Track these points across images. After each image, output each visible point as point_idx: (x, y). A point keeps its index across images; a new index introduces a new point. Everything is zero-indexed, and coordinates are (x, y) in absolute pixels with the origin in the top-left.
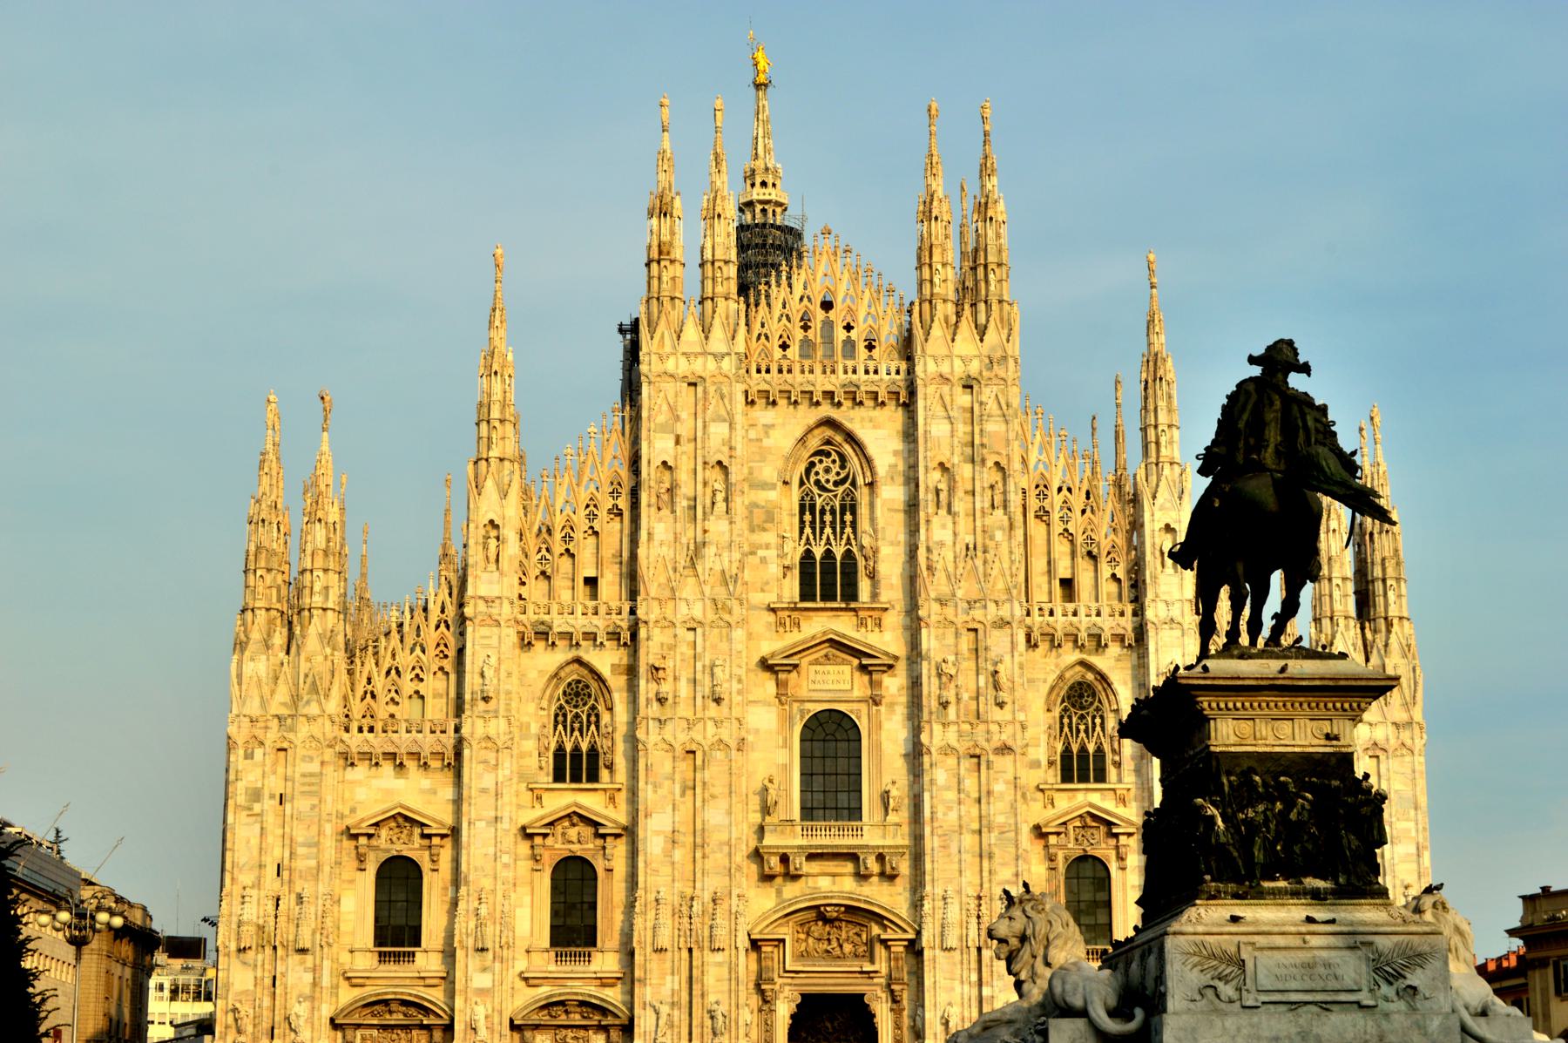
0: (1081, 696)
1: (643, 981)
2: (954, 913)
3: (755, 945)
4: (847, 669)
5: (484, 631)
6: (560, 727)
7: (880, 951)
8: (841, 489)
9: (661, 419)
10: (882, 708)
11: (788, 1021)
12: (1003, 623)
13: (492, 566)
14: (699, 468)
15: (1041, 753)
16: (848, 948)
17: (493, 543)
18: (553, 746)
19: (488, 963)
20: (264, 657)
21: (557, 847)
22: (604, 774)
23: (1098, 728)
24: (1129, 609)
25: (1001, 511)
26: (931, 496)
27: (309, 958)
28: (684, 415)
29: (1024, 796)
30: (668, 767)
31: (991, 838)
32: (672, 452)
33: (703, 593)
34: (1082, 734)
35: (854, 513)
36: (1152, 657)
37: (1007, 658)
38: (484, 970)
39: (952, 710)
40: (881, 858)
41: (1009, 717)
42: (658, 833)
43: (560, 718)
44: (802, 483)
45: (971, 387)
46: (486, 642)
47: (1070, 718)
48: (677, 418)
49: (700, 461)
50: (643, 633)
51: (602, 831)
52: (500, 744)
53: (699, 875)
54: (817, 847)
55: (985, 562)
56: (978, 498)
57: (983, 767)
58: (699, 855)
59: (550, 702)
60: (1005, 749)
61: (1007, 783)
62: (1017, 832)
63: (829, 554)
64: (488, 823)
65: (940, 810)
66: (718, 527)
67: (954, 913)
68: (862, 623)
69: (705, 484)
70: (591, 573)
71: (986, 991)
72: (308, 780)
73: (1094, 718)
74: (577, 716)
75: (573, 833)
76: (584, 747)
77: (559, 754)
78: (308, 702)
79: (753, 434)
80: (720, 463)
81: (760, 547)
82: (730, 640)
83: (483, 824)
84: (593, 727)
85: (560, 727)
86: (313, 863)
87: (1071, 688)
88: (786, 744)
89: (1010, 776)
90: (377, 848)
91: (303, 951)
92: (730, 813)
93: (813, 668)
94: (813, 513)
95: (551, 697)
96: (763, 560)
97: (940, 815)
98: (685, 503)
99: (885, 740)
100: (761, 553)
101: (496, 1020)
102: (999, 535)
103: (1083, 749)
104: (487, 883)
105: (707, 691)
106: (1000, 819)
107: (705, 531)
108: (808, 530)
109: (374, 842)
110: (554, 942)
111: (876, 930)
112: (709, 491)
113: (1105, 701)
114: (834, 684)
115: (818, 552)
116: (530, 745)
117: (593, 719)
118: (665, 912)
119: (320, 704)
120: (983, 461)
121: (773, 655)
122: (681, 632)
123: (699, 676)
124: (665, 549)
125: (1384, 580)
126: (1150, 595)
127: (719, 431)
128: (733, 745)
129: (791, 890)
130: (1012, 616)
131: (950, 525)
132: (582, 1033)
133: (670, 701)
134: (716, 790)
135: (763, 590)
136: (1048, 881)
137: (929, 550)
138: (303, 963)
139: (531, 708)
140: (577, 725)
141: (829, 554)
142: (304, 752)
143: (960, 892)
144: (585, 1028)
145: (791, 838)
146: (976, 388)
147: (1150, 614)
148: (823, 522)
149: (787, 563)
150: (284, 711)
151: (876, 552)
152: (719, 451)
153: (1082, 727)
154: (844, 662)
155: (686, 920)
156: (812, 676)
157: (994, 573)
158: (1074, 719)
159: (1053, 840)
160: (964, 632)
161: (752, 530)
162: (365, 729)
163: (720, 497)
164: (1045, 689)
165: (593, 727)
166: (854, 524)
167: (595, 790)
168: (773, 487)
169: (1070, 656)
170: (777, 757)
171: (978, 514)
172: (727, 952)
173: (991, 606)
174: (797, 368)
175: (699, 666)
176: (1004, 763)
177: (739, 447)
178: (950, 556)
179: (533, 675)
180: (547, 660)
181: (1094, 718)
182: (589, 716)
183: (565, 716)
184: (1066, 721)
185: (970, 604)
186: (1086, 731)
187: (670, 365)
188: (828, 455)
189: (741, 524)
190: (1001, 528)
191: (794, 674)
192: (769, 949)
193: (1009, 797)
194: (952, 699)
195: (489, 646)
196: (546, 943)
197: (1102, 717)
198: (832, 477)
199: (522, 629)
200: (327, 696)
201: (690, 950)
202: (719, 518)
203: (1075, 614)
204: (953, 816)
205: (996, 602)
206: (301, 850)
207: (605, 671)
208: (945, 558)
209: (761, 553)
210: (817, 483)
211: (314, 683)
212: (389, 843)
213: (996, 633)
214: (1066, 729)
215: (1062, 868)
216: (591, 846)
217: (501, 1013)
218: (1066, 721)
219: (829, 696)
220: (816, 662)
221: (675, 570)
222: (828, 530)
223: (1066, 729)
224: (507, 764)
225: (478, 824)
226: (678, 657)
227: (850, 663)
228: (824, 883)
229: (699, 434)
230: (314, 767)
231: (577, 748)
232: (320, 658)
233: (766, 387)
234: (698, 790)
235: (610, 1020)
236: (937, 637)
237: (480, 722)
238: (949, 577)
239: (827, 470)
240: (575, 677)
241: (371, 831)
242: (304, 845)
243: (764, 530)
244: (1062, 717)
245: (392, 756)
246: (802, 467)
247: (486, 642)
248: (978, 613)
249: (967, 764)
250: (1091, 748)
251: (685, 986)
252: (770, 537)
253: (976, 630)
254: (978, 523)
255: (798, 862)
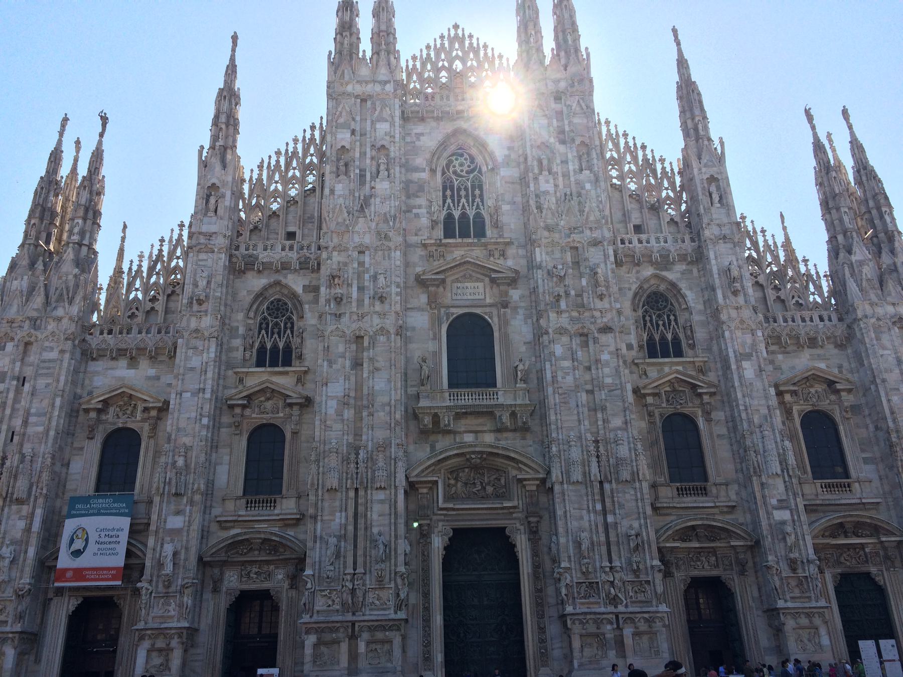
0: (657, 302)
1: (314, 518)
2: (576, 454)
3: (412, 487)
4: (481, 285)
5: (203, 256)
6: (263, 332)
7: (515, 489)
8: (472, 175)
9: (341, 120)
10: (508, 311)
11: (442, 552)
12: (596, 243)
13: (211, 214)
14: (368, 150)
15: (633, 339)
16: (490, 489)
17: (212, 200)
18: (257, 345)
19: (182, 507)
20: (26, 277)
21: (255, 417)
22: (295, 362)
23: (673, 323)
24: (687, 238)
25: (587, 172)
26: (535, 163)
27: (25, 507)
28: (358, 118)
29: (625, 362)
30: (341, 348)
31: (601, 395)
32: (349, 140)
33: (369, 228)
34: (661, 327)
35: (481, 188)
36: (713, 262)
37: (602, 265)
38: (178, 513)
39: (563, 305)
40: (513, 415)
41: (607, 306)
42: (332, 398)
43: (264, 326)
44: (443, 173)
45: (561, 99)
46: (201, 263)
47: (650, 316)
48: (354, 119)
49: (368, 145)
50: (324, 255)
51: (289, 401)
52: (206, 334)
53: (365, 430)
54: (462, 407)
55: (580, 203)
56: (570, 163)
57: (591, 343)
58: (365, 414)
59: (255, 313)
60: (606, 329)
61: (610, 353)
62: (622, 388)
63: (464, 216)
64: (193, 394)
65: (560, 374)
66: (382, 186)
67: (576, 454)
68: (491, 255)
69: (372, 158)
70: (291, 229)
71: (610, 519)
72: (47, 365)
73: (668, 316)
74: (277, 324)
75: (269, 405)
76: (281, 345)
77: (262, 350)
78: (55, 308)
79: (408, 139)
80: (383, 146)
81: (415, 207)
82: (389, 258)
83: (189, 394)
84: (289, 331)
85: (263, 332)
86: (40, 429)
87: (648, 297)
88: (436, 337)
89: (612, 348)
90: (106, 421)
91: (20, 502)
92: (389, 381)
93: (455, 285)
94: (452, 190)
95: (257, 309)
96: (417, 216)
97: (559, 379)
98: (357, 171)
99: (514, 334)
100: (414, 211)
101: (182, 557)
102: (588, 186)
103: (663, 338)
104: (187, 440)
105: (372, 292)
106: (608, 380)
107: (373, 188)
108: (449, 201)
109: (104, 417)
110: (245, 492)
111: (514, 472)
112: (374, 163)
113: (676, 304)
114: (472, 294)
115: (457, 214)
116: (237, 342)
117: (289, 325)
118: (333, 461)
119: (64, 307)
120: (573, 140)
121: (424, 273)
122: (355, 254)
123: (366, 284)
124: (341, 199)
125: (879, 208)
126: (705, 220)
127: (383, 127)
128: (392, 330)
129: (442, 442)
130: (603, 237)
131: (552, 181)
132: (265, 568)
133: (345, 301)
134: (377, 365)
135: (416, 235)
136: (648, 432)
137: (537, 196)
138: (19, 512)
139: (240, 316)
140: (276, 330)
141: (464, 216)
142: (47, 344)
143: (580, 438)
144: (268, 562)
145: (441, 399)
146: (563, 98)
147: (707, 233)
148: (459, 196)
149: (435, 218)
150: (35, 314)
151: (497, 209)
152: (383, 139)
153: (661, 323)
154: (478, 280)
155: (352, 465)
156: (454, 291)
157: (586, 210)
158: (654, 317)
159: (650, 400)
160: (568, 249)
161: (408, 197)
162: (106, 331)
163: (382, 167)
164: (630, 294)
165: (289, 331)
166: (481, 196)
167: (286, 373)
168: (424, 170)
169: (648, 271)
170: (431, 345)
171: (572, 173)
172: (388, 492)
173: (588, 232)
174: (437, 97)
175: (367, 276)
176: (605, 338)
177: (397, 136)
178: (554, 200)
179: (245, 293)
180: (256, 282)
181: (668, 316)
182: (286, 324)
183: (268, 324)
184: (648, 318)
185: (572, 230)
186: (664, 325)
187: (349, 88)
188: (462, 155)
189: (398, 186)
190: (591, 182)
191: (441, 289)
192: (425, 491)
193: (613, 364)
194: (562, 294)
195: (204, 266)
196: (240, 492)
197: (674, 315)
198: (465, 168)
199: (234, 260)
200: (70, 303)
201: (357, 490)
202: (382, 180)
203: (648, 242)
204: (570, 379)
205: (591, 229)
206: (32, 419)
207: (299, 290)
208: (550, 202)
209: (414, 211)
210: (455, 173)
211: (61, 295)
212: (114, 419)
213: (592, 249)
214: (649, 324)
215: (659, 424)
216: (281, 415)
217: (187, 549)
218: (648, 318)
219: (467, 303)
220: (457, 280)
221: (349, 213)
222: (463, 200)
223: (649, 324)
224: (213, 349)
225: (184, 395)
226: (351, 271)
227: (482, 281)
228: (469, 438)
229: (368, 129)
230: (54, 355)
231: (275, 347)
232: (70, 277)
233: (417, 109)
234: (365, 365)
235: (288, 555)
236: (547, 253)
237: (193, 319)
238: (553, 214)
239: (461, 165)
240: (277, 297)
241: (100, 406)
242: (35, 415)
243: (417, 197)
244: (644, 317)
245: (121, 353)
246: (443, 162)
247: (201, 263)
248: (576, 237)
249: (576, 341)
250: (669, 337)
251: (351, 519)
252: (422, 201)
253: (577, 248)
254: (572, 179)
255: (446, 419)
